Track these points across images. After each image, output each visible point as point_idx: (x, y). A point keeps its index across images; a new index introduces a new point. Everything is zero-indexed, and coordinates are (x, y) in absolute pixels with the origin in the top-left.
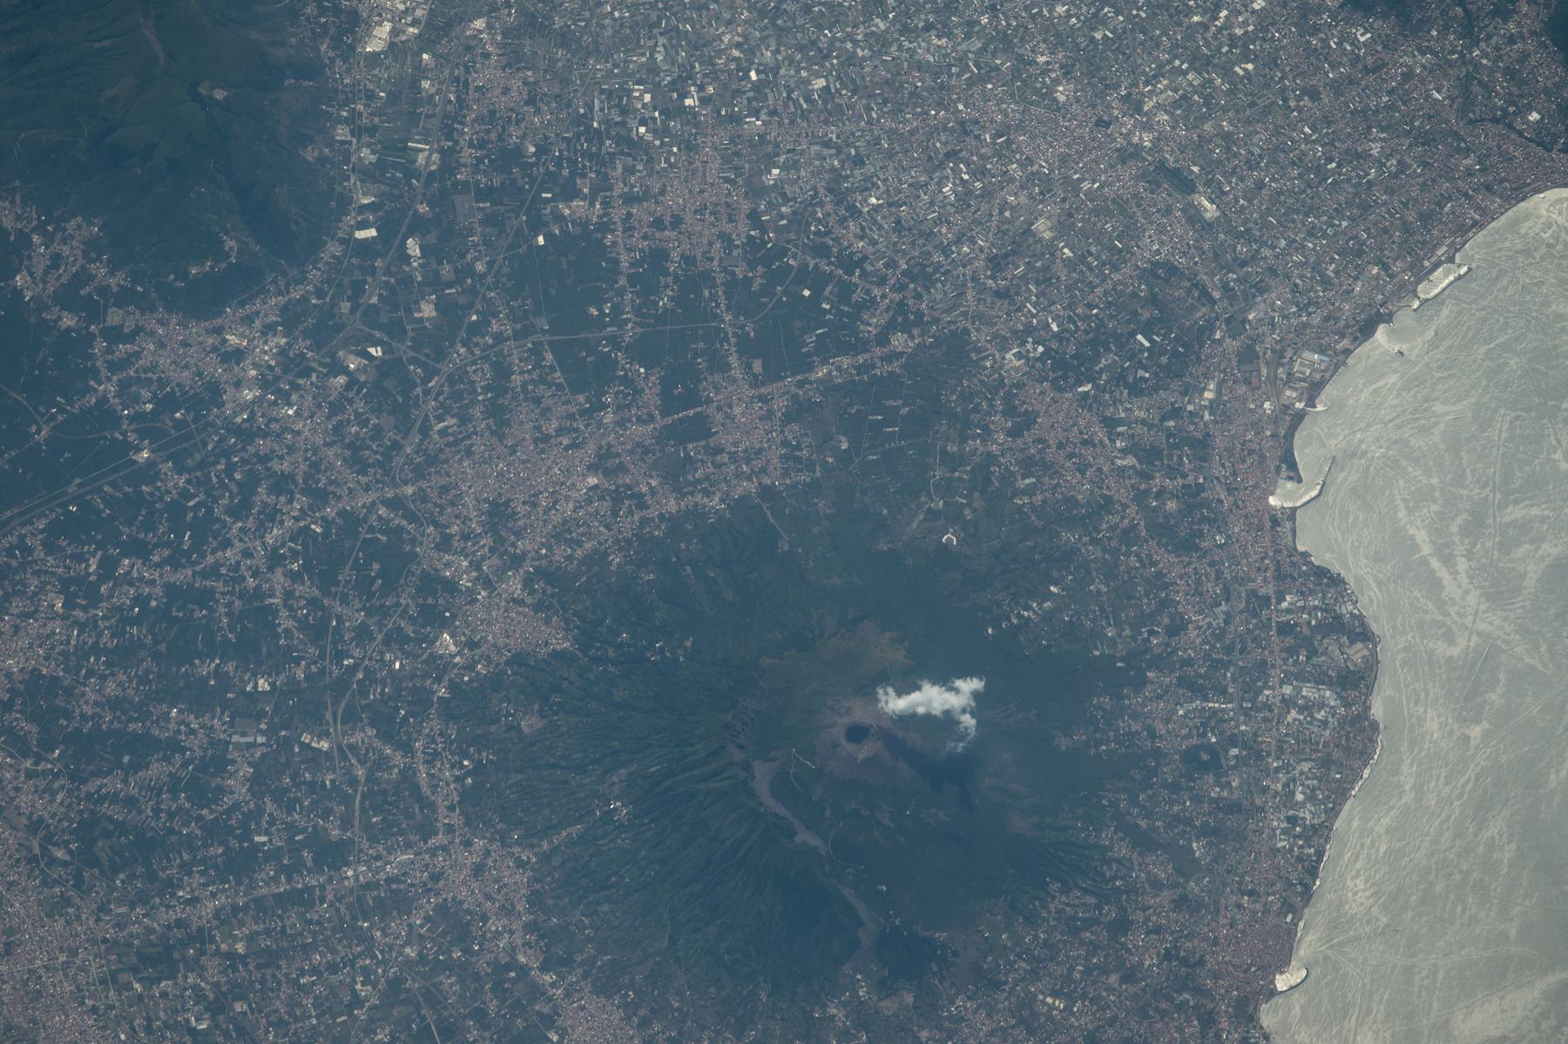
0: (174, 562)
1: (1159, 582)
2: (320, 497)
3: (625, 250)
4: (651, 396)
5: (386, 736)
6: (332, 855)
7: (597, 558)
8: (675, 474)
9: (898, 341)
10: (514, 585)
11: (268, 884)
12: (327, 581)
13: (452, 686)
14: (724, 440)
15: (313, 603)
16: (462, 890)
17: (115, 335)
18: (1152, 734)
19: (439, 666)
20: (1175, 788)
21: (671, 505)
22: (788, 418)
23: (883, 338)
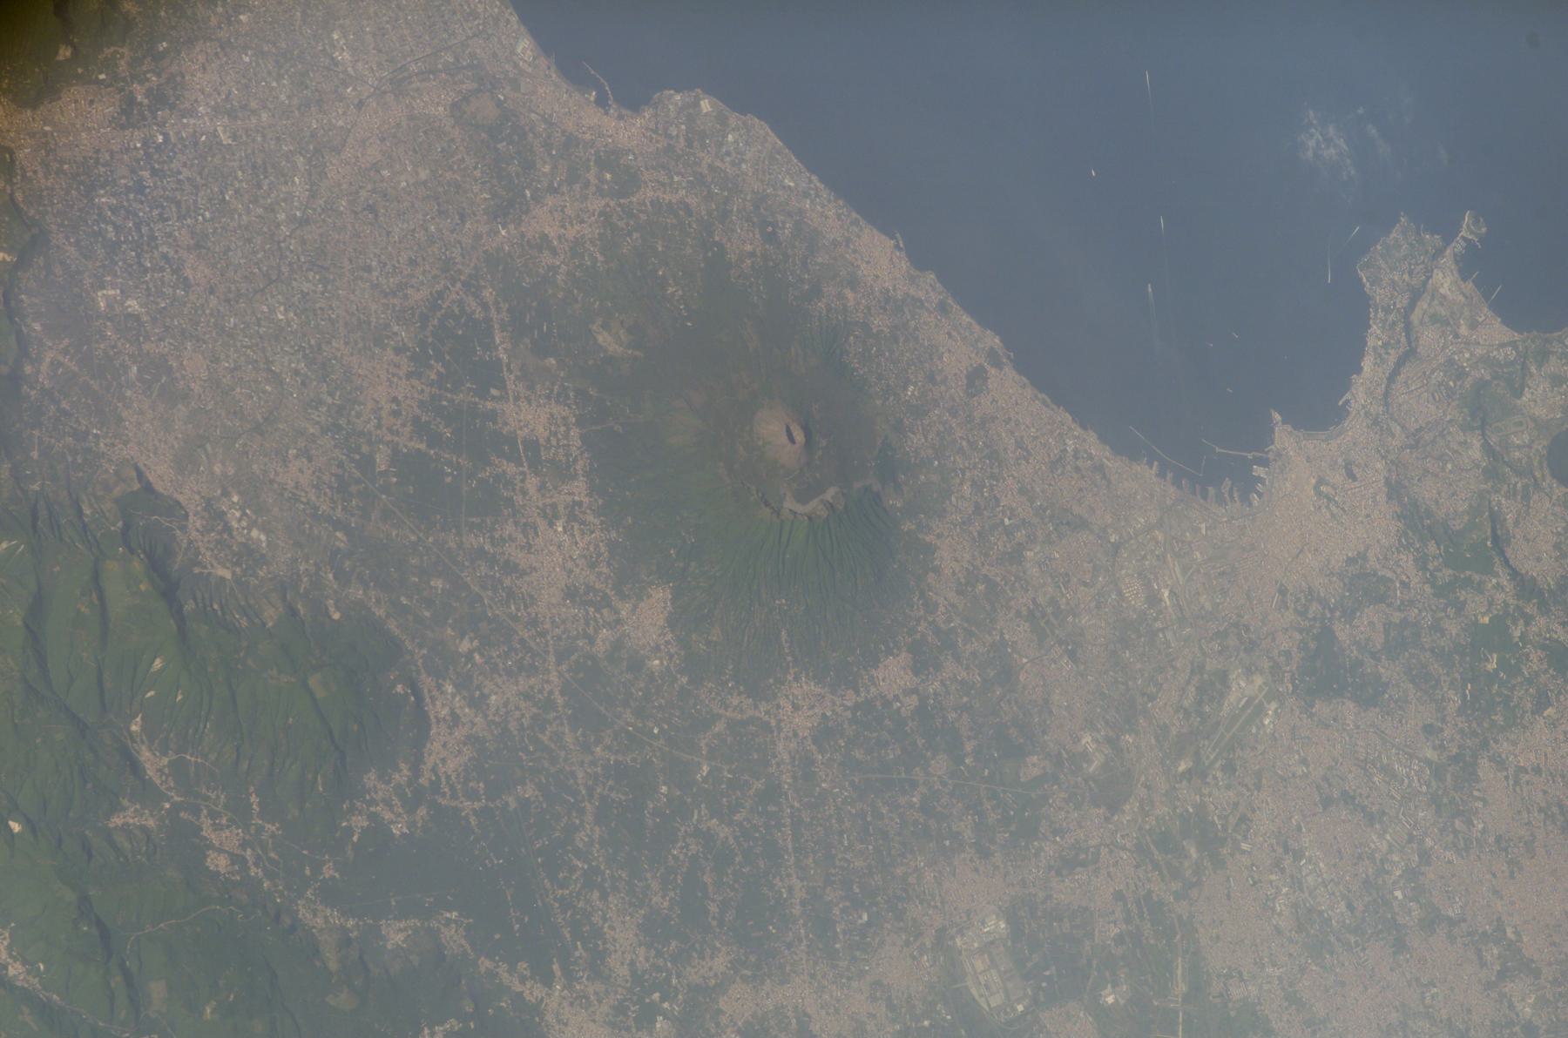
4: (511, 469)
23: (485, 306)
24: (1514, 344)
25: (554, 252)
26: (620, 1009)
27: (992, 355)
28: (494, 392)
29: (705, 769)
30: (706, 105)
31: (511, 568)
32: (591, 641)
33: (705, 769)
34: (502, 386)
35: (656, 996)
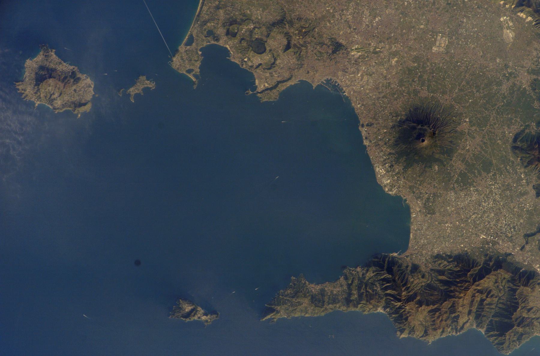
0: (498, 107)
2: (490, 125)
3: (484, 174)
4: (469, 161)
6: (461, 90)
7: (461, 140)
9: (452, 186)
10: (466, 131)
11: (464, 83)
14: (460, 162)
15: (483, 114)
16: (447, 97)
17: (522, 126)
18: (398, 165)
19: (466, 117)
20: (392, 162)
21: (459, 151)
24: (256, 72)
25: (434, 185)
26: (515, 77)
28: (463, 172)
29: (470, 101)
30: (387, 190)
31: (482, 147)
32: (476, 130)
33: (470, 101)
34: (461, 172)
35: (507, 75)
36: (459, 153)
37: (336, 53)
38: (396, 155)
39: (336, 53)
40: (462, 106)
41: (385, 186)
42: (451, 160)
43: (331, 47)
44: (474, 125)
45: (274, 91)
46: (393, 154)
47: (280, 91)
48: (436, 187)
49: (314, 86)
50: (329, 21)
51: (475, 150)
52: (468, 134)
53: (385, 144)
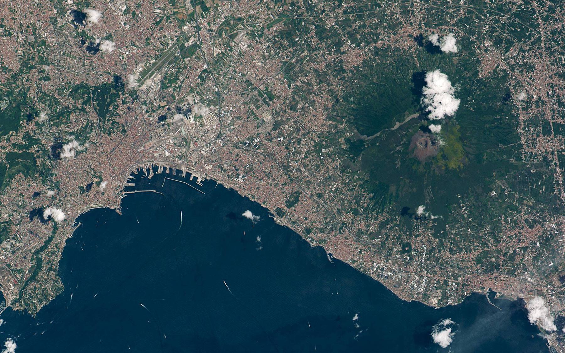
1: (468, 250)
2: (545, 19)
5: (461, 20)
8: (533, 122)
10: (504, 66)
12: (517, 15)
13: (473, 42)
14: (541, 138)
15: (510, 10)
18: (417, 236)
19: (481, 39)
20: (398, 238)
22: (545, 158)
27: (281, 213)
32: (522, 50)
36: (525, 121)
37: (108, 111)
38: (396, 219)
39: (108, 111)
40: (454, 25)
41: (426, 295)
42: (521, 146)
43: (88, 108)
44: (509, 44)
45: (43, 275)
46: (387, 222)
47: (54, 267)
48: (534, 221)
49: (116, 206)
50: (44, 62)
51: (554, 92)
52: (513, 69)
53: (356, 213)
